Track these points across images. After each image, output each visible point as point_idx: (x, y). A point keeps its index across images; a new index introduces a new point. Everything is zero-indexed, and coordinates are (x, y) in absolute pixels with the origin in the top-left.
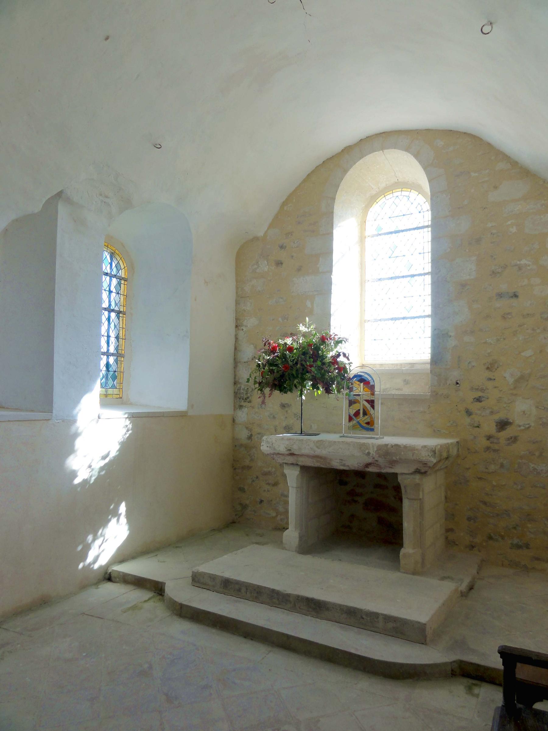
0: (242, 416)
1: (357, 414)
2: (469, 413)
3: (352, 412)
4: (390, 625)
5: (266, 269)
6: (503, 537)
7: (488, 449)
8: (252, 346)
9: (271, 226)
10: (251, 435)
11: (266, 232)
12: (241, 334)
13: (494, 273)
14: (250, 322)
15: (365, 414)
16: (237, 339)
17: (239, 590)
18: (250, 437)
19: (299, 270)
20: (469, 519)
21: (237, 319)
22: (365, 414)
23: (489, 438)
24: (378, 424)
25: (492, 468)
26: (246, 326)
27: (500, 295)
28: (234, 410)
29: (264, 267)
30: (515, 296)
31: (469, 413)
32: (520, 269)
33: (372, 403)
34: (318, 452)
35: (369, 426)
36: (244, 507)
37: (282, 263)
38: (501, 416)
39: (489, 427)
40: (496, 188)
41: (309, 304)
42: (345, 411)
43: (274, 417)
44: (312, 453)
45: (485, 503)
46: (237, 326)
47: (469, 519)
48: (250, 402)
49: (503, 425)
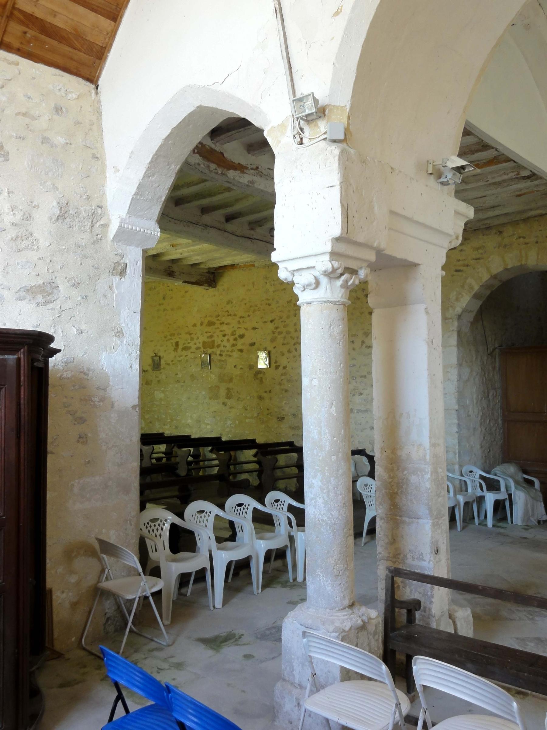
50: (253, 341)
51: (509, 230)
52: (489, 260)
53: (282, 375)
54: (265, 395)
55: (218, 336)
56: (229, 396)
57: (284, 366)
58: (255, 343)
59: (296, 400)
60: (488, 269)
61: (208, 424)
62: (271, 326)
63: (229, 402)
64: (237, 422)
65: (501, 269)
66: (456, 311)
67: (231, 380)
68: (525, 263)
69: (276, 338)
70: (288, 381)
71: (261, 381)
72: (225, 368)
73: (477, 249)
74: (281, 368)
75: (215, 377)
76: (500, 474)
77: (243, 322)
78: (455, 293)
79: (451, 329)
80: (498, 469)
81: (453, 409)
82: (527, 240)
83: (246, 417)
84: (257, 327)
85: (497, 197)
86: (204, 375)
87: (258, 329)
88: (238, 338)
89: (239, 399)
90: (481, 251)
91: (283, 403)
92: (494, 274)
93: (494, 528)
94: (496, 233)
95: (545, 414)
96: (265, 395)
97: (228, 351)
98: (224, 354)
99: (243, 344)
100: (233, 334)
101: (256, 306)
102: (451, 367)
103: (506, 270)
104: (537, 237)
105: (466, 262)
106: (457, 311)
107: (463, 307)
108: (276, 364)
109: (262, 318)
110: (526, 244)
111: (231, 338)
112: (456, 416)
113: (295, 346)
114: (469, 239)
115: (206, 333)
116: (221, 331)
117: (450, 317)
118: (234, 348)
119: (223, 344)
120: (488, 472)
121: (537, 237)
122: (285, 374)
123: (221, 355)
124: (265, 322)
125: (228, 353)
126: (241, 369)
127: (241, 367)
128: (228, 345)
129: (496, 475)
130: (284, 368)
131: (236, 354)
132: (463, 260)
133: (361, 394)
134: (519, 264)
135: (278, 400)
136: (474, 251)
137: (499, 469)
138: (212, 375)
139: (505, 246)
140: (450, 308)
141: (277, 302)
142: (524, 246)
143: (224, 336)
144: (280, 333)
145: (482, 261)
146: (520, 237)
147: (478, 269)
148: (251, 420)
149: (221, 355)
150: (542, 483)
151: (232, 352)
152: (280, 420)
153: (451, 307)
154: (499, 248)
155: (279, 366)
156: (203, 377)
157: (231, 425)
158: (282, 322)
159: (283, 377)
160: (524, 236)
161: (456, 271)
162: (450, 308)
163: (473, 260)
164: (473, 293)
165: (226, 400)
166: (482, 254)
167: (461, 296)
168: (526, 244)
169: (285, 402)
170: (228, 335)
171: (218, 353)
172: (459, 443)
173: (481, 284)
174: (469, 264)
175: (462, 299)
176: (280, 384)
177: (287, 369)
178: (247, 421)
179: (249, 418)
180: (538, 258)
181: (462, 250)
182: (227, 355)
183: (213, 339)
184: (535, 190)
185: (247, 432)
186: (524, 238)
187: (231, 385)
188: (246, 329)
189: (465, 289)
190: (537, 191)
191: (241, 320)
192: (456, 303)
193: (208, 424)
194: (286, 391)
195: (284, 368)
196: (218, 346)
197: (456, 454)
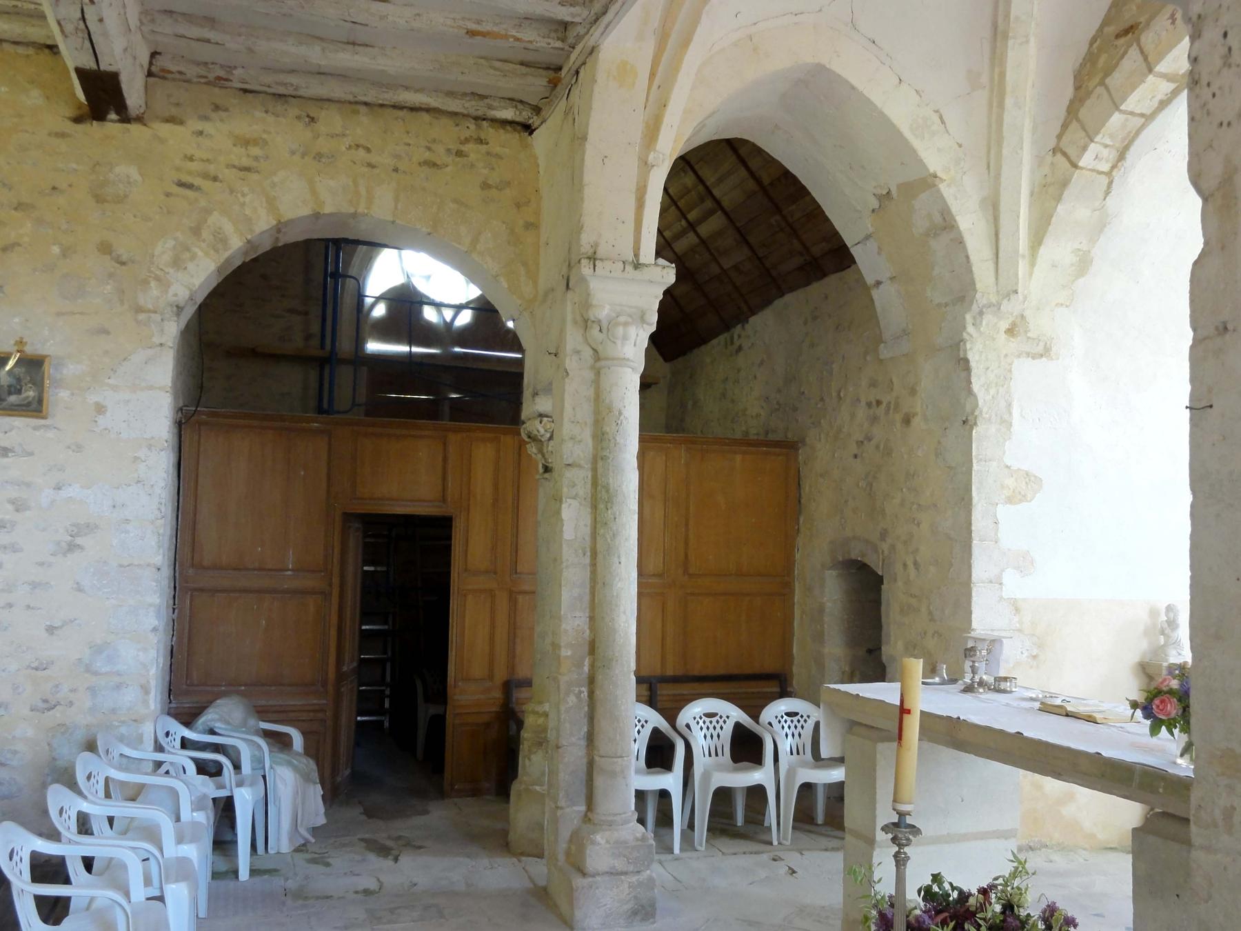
51: (331, 120)
52: (276, 179)
60: (271, 204)
65: (305, 211)
66: (171, 292)
68: (366, 211)
73: (246, 142)
76: (226, 730)
78: (170, 243)
79: (156, 340)
80: (209, 717)
81: (148, 565)
82: (374, 158)
85: (418, 15)
90: (255, 151)
92: (286, 219)
93: (257, 879)
94: (298, 118)
95: (289, 573)
102: (150, 447)
103: (317, 216)
104: (397, 157)
105: (212, 169)
106: (176, 295)
107: (195, 286)
110: (371, 166)
112: (155, 584)
114: (226, 110)
117: (150, 307)
120: (188, 724)
121: (397, 157)
129: (212, 732)
132: (203, 160)
134: (352, 210)
136: (234, 145)
137: (216, 716)
139: (319, 156)
140: (153, 284)
142: (366, 170)
145: (254, 177)
146: (358, 146)
147: (244, 195)
150: (305, 734)
153: (158, 279)
154: (303, 155)
160: (369, 146)
161: (181, 184)
162: (153, 284)
163: (234, 170)
164: (227, 254)
166: (256, 159)
167: (188, 255)
168: (371, 166)
172: (157, 660)
173: (249, 237)
174: (220, 177)
175: (191, 266)
180: (396, 208)
181: (201, 133)
184: (514, 33)
186: (368, 150)
189: (204, 241)
190: (517, 39)
192: (171, 271)
197: (146, 691)
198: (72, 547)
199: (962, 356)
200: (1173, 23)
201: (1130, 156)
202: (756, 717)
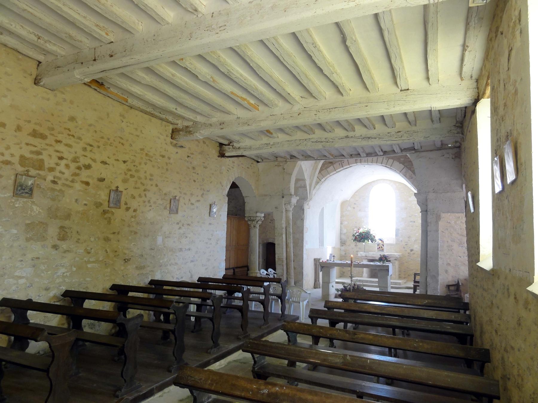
0: (343, 248)
1: (379, 248)
2: (404, 248)
3: (378, 247)
4: (394, 283)
5: (350, 209)
6: (411, 275)
7: (408, 256)
8: (346, 230)
9: (351, 198)
10: (346, 253)
11: (350, 199)
12: (342, 226)
13: (410, 216)
14: (346, 223)
15: (382, 247)
16: (341, 227)
17: (363, 282)
18: (345, 254)
19: (360, 210)
20: (404, 272)
21: (341, 222)
22: (382, 247)
23: (409, 253)
24: (385, 250)
25: (409, 260)
26: (344, 224)
27: (411, 222)
28: (341, 246)
29: (349, 208)
30: (414, 222)
31: (404, 248)
32: (415, 216)
33: (383, 245)
34: (373, 256)
35: (383, 250)
36: (344, 272)
37: (355, 208)
38: (412, 248)
39: (409, 251)
40: (410, 197)
41: (363, 219)
42: (376, 247)
43: (353, 249)
44: (371, 256)
45: (408, 268)
46: (341, 224)
47: (404, 272)
48: (345, 244)
49: (412, 250)
50: (103, 176)
53: (132, 217)
54: (111, 236)
55: (50, 155)
56: (63, 238)
57: (135, 208)
58: (104, 179)
59: (143, 242)
61: (21, 277)
62: (123, 166)
63: (64, 245)
64: (74, 269)
67: (68, 216)
69: (128, 180)
70: (138, 223)
71: (109, 222)
72: (59, 201)
74: (131, 210)
75: (41, 211)
77: (91, 151)
83: (89, 262)
84: (108, 162)
86: (17, 206)
87: (109, 164)
88: (83, 168)
89: (78, 241)
91: (132, 245)
96: (111, 236)
97: (67, 180)
98: (59, 182)
99: (88, 177)
100: (75, 160)
101: (109, 139)
108: (126, 206)
109: (114, 154)
111: (73, 166)
113: (145, 192)
115: (27, 144)
116: (57, 151)
118: (76, 178)
119: (58, 168)
122: (134, 217)
123: (54, 182)
124: (118, 160)
125: (68, 183)
126: (85, 205)
127: (85, 202)
128: (68, 173)
130: (135, 211)
131: (78, 186)
133: (186, 237)
135: (126, 242)
138: (35, 207)
141: (131, 145)
143: (61, 158)
144: (132, 176)
148: (94, 264)
149: (54, 182)
151: (73, 181)
152: (126, 262)
155: (130, 208)
156: (16, 207)
157: (65, 274)
158: (134, 166)
159: (133, 220)
165: (59, 243)
169: (133, 243)
170: (67, 159)
171: (50, 178)
176: (129, 226)
177: (137, 212)
178: (89, 266)
179: (93, 262)
182: (64, 185)
183: (40, 157)
185: (88, 279)
187: (67, 223)
188: (94, 161)
191: (89, 148)
193: (21, 277)
194: (136, 233)
195: (135, 211)
196: (51, 170)
198: (217, 243)
199: (303, 208)
200: (340, 165)
201: (326, 180)
202: (268, 272)
